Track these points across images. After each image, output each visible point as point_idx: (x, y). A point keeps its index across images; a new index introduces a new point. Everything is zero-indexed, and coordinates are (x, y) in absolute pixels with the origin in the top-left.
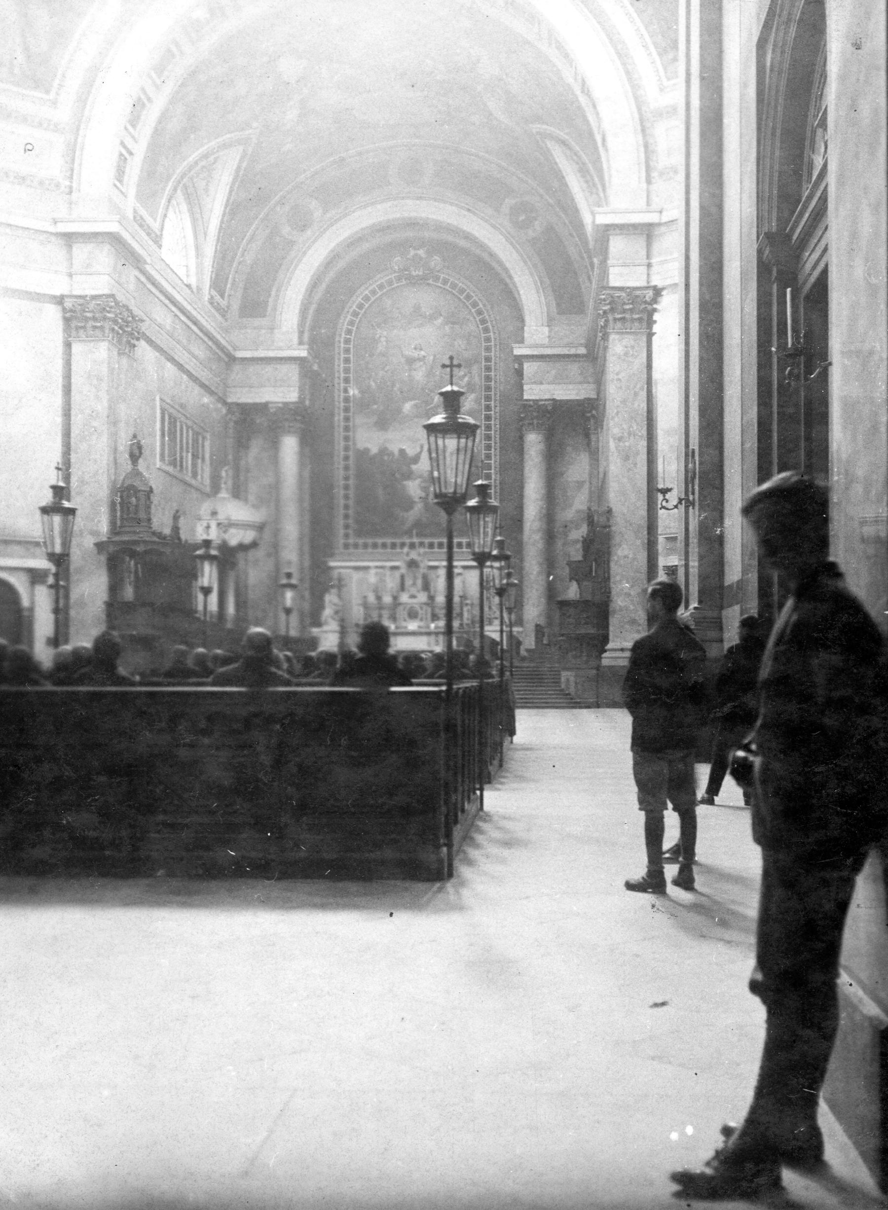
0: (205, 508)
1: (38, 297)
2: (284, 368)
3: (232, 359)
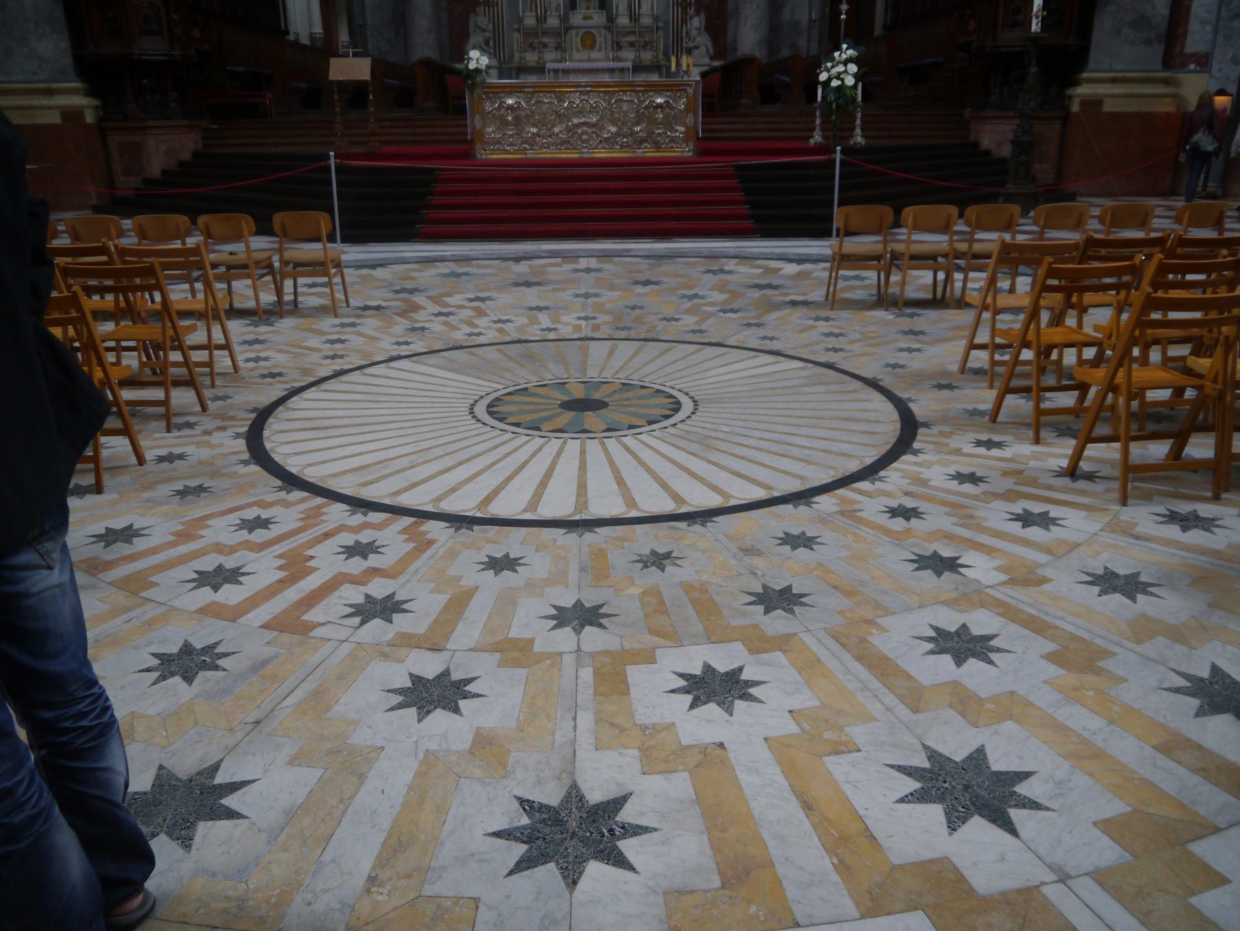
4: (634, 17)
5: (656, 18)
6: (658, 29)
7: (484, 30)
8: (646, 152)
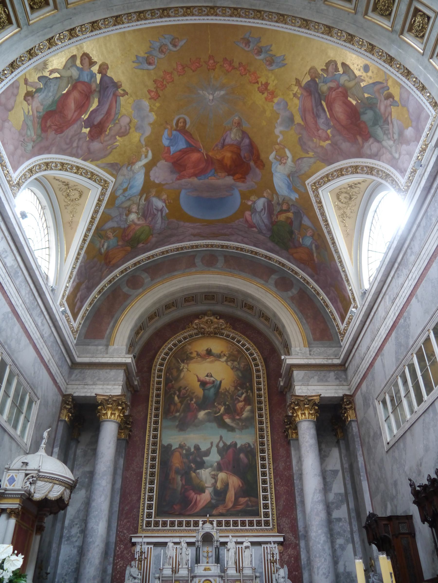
2: (113, 373)
4: (239, 570)
5: (254, 570)
6: (256, 577)
7: (135, 578)
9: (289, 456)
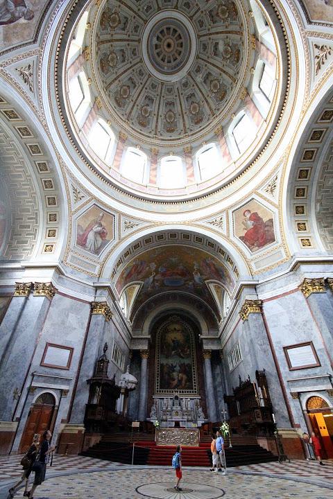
0: (123, 376)
1: (86, 302)
2: (144, 341)
3: (132, 338)
4: (187, 409)
8: (189, 445)
9: (202, 368)
